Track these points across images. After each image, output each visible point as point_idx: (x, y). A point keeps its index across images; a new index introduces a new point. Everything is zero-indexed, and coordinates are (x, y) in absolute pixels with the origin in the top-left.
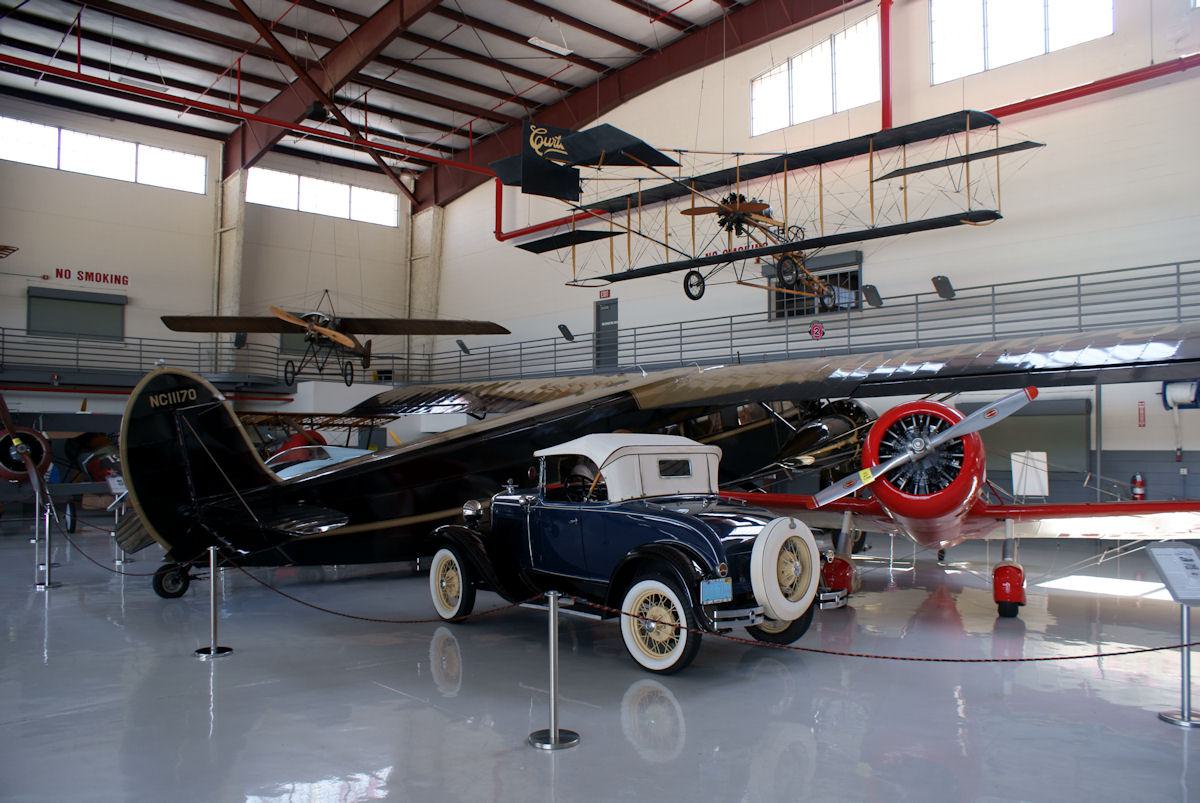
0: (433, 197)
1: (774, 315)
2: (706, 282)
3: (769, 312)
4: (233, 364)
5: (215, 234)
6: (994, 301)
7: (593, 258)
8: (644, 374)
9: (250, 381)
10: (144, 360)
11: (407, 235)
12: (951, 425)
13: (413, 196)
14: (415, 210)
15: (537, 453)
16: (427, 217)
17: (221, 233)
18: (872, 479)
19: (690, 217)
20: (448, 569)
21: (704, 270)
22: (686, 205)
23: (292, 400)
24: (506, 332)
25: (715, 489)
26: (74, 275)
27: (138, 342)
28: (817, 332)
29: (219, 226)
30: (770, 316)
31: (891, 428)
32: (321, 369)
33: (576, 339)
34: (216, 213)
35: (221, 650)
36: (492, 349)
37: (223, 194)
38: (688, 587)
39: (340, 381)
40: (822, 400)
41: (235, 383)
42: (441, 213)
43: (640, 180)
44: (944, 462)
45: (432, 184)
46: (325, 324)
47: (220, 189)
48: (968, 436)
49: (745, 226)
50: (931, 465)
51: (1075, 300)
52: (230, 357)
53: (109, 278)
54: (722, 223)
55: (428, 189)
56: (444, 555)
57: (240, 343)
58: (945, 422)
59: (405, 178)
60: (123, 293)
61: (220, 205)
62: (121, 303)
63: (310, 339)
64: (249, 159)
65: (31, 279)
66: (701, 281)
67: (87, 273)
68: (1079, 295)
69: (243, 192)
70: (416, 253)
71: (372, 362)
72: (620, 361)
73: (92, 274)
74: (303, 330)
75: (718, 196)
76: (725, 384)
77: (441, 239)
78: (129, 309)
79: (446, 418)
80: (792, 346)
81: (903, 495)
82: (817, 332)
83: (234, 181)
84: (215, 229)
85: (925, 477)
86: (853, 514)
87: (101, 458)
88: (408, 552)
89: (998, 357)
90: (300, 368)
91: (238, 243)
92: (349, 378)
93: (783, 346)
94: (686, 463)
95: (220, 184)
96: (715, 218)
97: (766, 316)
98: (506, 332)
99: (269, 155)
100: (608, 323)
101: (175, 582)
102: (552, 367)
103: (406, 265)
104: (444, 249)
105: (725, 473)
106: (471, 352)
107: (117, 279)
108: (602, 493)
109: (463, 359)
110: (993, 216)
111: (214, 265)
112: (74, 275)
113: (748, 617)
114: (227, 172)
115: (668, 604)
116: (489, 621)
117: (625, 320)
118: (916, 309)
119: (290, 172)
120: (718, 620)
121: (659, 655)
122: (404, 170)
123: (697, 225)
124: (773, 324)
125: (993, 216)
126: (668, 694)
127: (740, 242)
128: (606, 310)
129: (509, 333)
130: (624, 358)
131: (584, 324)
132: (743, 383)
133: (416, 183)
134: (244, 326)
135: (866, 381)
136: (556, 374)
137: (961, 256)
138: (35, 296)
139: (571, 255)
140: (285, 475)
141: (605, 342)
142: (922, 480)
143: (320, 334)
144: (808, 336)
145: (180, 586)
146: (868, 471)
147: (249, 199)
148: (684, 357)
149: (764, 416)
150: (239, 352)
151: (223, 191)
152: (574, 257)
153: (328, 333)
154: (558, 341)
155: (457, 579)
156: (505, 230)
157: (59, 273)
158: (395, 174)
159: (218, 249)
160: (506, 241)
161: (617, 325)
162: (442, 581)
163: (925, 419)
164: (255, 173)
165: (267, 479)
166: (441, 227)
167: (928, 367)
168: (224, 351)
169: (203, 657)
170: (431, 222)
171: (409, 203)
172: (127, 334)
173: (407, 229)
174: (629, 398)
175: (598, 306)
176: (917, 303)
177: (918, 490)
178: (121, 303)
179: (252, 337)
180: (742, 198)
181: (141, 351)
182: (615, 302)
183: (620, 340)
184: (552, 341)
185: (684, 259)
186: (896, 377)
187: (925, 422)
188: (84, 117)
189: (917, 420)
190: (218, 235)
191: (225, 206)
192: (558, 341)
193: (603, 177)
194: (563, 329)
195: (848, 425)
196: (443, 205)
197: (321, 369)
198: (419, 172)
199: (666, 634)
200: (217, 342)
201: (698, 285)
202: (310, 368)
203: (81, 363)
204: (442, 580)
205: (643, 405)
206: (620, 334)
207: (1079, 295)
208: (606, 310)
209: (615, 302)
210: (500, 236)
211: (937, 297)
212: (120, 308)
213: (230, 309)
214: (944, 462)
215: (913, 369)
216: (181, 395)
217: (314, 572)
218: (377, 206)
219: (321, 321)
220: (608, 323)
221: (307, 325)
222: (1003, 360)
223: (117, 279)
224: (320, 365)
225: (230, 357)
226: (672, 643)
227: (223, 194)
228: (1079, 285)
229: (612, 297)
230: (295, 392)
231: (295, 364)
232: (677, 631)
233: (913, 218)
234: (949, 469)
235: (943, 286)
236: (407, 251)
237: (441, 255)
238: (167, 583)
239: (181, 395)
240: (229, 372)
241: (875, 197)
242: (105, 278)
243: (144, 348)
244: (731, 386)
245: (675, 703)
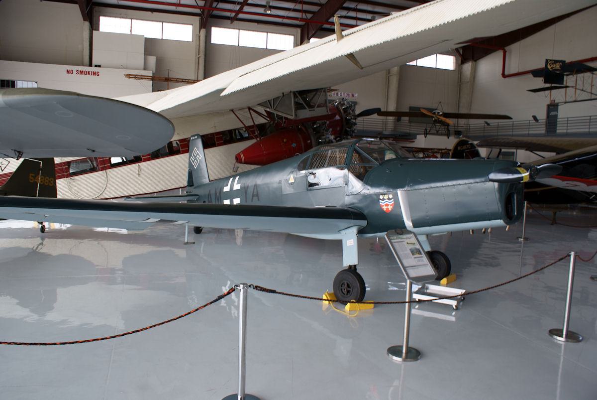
16: (468, 67)
23: (414, 142)
32: (437, 132)
33: (539, 121)
41: (394, 135)
72: (558, 131)
130: (560, 130)
131: (542, 115)
141: (552, 122)
143: (439, 119)
150: (398, 123)
156: (506, 73)
161: (557, 115)
166: (474, 71)
175: (549, 106)
194: (535, 118)
196: (476, 61)
197: (437, 132)
202: (433, 131)
206: (558, 120)
208: (553, 107)
210: (504, 75)
224: (437, 129)
230: (416, 138)
231: (427, 128)
237: (474, 81)
240: (391, 131)
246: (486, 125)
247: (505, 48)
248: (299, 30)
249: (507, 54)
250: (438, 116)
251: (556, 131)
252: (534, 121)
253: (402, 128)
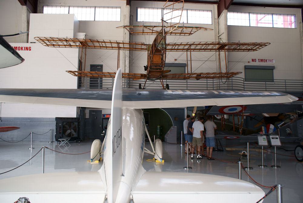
10: (287, 88)
26: (257, 60)
27: (284, 81)
62: (272, 68)
65: (245, 63)
67: (261, 59)
73: (262, 60)
78: (274, 71)
112: (257, 60)
138: (246, 68)
157: (253, 60)
172: (274, 79)
181: (266, 86)
188: (252, 8)
203: (287, 90)
243: (287, 83)
248: (216, 6)
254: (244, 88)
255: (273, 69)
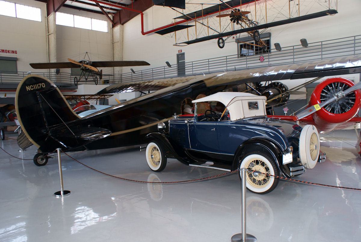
0: (119, 21)
1: (239, 56)
2: (225, 42)
3: (238, 55)
4: (56, 80)
5: (46, 36)
6: (322, 47)
7: (182, 35)
8: (204, 75)
9: (62, 85)
11: (111, 35)
12: (351, 86)
13: (113, 21)
14: (114, 25)
15: (193, 102)
16: (118, 28)
17: (48, 35)
18: (320, 108)
19: (219, 18)
20: (154, 150)
21: (224, 38)
22: (218, 14)
23: (76, 91)
24: (149, 64)
25: (266, 115)
28: (262, 60)
29: (47, 33)
30: (238, 56)
31: (324, 89)
32: (86, 80)
33: (172, 66)
34: (46, 28)
35: (66, 192)
36: (142, 71)
37: (48, 22)
38: (275, 156)
39: (94, 84)
40: (261, 83)
42: (122, 27)
43: (202, 4)
44: (347, 101)
45: (119, 18)
46: (87, 64)
47: (47, 20)
48: (357, 91)
49: (240, 22)
50: (342, 102)
51: (353, 45)
52: (55, 78)
53: (10, 52)
54: (231, 20)
55: (117, 19)
56: (152, 145)
57: (58, 72)
58: (346, 84)
59: (110, 15)
60: (16, 57)
61: (47, 25)
62: (15, 60)
63: (83, 69)
64: (56, 9)
66: (223, 42)
67: (2, 50)
68: (355, 43)
69: (55, 20)
70: (114, 41)
71: (103, 77)
72: (186, 73)
73: (4, 50)
74: (79, 66)
75: (229, 12)
76: (231, 78)
77: (123, 35)
78: (18, 62)
79: (129, 95)
80: (248, 65)
81: (329, 114)
82: (262, 60)
83: (51, 17)
84: (46, 34)
85: (339, 107)
86: (300, 122)
87: (13, 113)
88: (135, 142)
89: (315, 66)
90: (79, 80)
91: (54, 38)
92: (96, 83)
93: (245, 66)
94: (256, 103)
95: (46, 18)
96: (229, 18)
97: (237, 56)
98: (148, 64)
99: (62, 8)
100: (181, 61)
101: (42, 159)
102: (164, 76)
103: (111, 45)
104: (124, 39)
105: (268, 110)
106: (136, 73)
107: (13, 52)
108: (227, 117)
109: (133, 75)
110: (334, 12)
111: (47, 46)
113: (303, 169)
114: (48, 14)
115: (263, 164)
116: (174, 169)
117: (188, 59)
118: (293, 51)
119: (70, 14)
120: (292, 172)
121: (259, 186)
122: (109, 13)
123: (221, 20)
124: (239, 59)
125: (334, 12)
126: (267, 205)
127: (237, 27)
128: (181, 56)
129: (149, 64)
131: (174, 61)
132: (238, 77)
133: (113, 17)
134: (58, 66)
135: (294, 73)
136: (165, 78)
137: (313, 31)
139: (174, 35)
140: (82, 116)
142: (338, 108)
143: (86, 67)
144: (259, 61)
145: (45, 161)
146: (318, 105)
147: (57, 23)
148: (210, 71)
149: (245, 89)
150: (58, 75)
151: (48, 20)
152: (175, 35)
153: (89, 67)
154: (165, 67)
155: (158, 155)
156: (145, 31)
158: (107, 14)
159: (48, 41)
160: (145, 35)
162: (152, 155)
163: (338, 84)
164: (58, 14)
165: (76, 118)
166: (122, 32)
167: (289, 71)
168: (52, 75)
169: (58, 197)
170: (119, 30)
171: (111, 23)
172: (18, 71)
173: (111, 33)
174: (203, 82)
175: (178, 55)
176: (294, 49)
177: (336, 112)
178: (15, 60)
179: (62, 70)
180: (239, 10)
182: (184, 54)
183: (186, 66)
184: (163, 68)
185: (216, 33)
186: (278, 74)
187: (338, 86)
189: (334, 85)
190: (47, 36)
191: (49, 26)
192: (165, 67)
193: (177, 10)
194: (167, 63)
195: (278, 92)
196: (123, 24)
198: (114, 13)
199: (261, 178)
200: (50, 73)
201: (222, 43)
203: (3, 81)
204: (152, 154)
205: (208, 85)
206: (186, 64)
207: (355, 43)
208: (181, 56)
209: (184, 54)
210: (143, 33)
211: (301, 46)
212: (15, 62)
213: (53, 60)
214: (347, 101)
215: (285, 72)
216: (39, 86)
217: (94, 152)
218: (101, 25)
219: (85, 63)
220: (181, 61)
221: (81, 64)
222: (317, 68)
223: (13, 52)
225: (55, 78)
226: (265, 181)
227: (48, 22)
228: (355, 40)
229: (183, 52)
230: (77, 88)
232: (268, 176)
233: (302, 15)
234: (348, 103)
235: (304, 42)
236: (111, 41)
238: (39, 161)
239: (39, 86)
241: (290, 7)
242: (9, 52)
244: (247, 77)
245: (270, 210)
246: (133, 73)
247: (143, 13)
249: (144, 16)
250: (84, 65)
251: (185, 73)
252: (168, 67)
253: (62, 80)
254: (2, 78)
255: (16, 61)
